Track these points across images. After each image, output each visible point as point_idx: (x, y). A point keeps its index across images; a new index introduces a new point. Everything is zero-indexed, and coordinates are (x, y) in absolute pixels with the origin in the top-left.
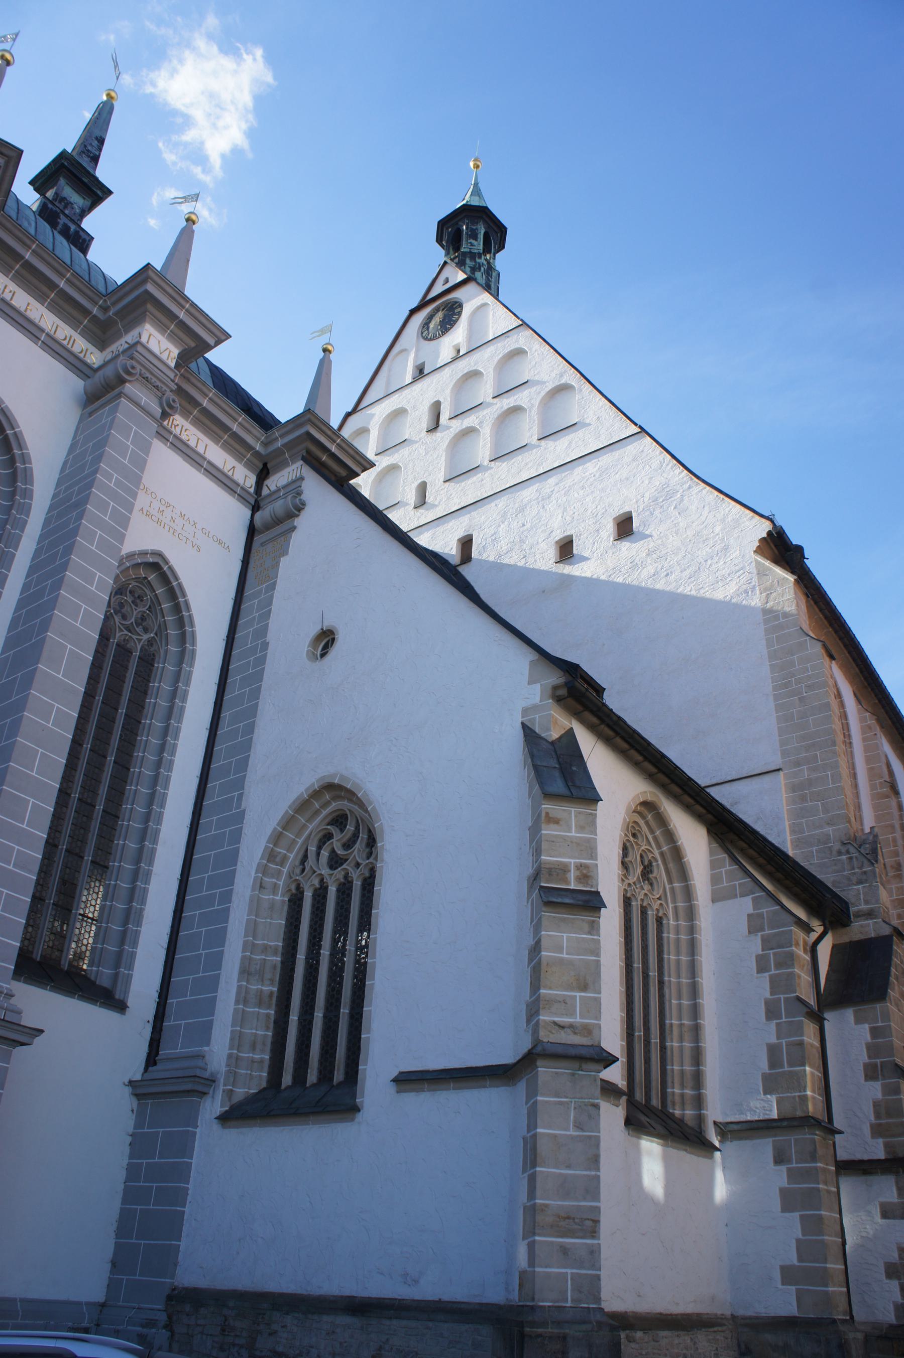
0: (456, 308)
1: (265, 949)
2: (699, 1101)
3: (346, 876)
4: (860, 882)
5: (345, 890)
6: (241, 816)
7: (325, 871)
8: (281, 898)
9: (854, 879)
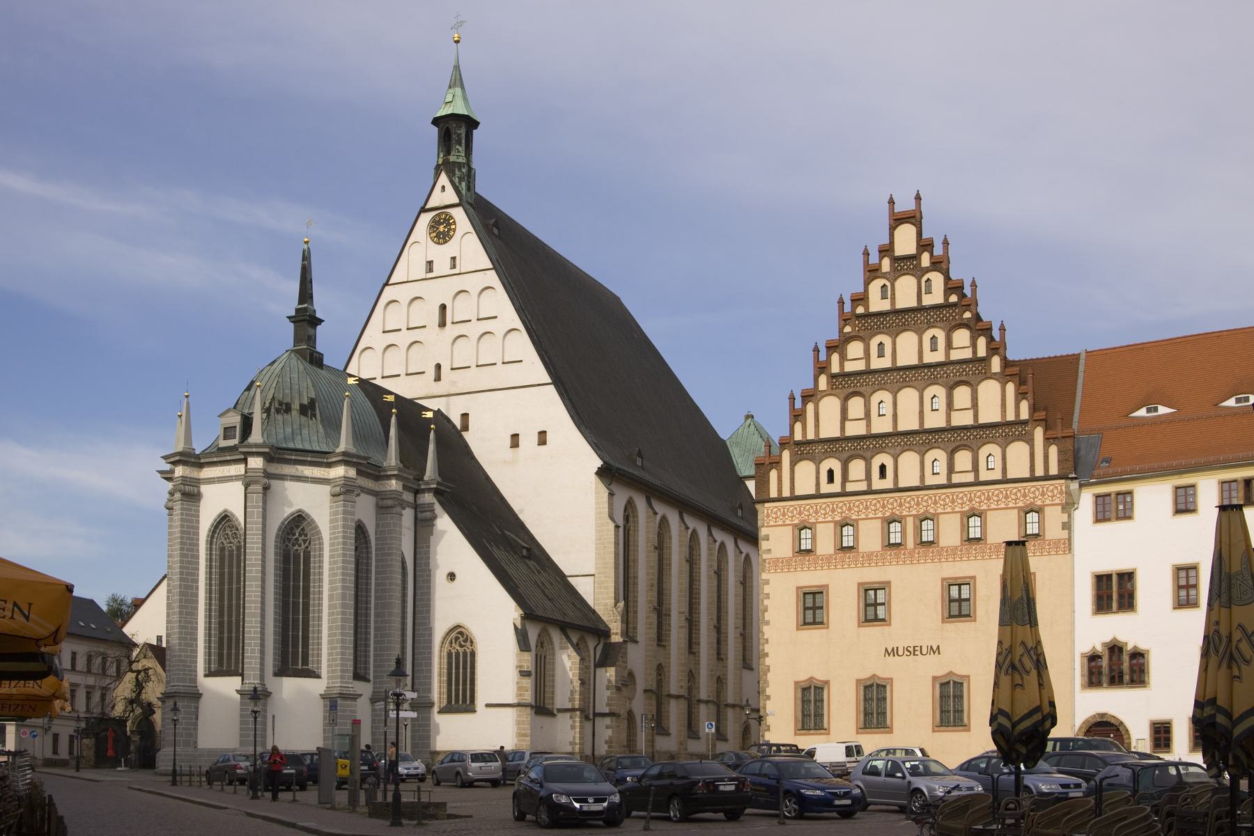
0: (451, 224)
2: (553, 704)
3: (465, 650)
4: (615, 622)
5: (465, 653)
7: (459, 648)
8: (445, 654)
9: (614, 621)
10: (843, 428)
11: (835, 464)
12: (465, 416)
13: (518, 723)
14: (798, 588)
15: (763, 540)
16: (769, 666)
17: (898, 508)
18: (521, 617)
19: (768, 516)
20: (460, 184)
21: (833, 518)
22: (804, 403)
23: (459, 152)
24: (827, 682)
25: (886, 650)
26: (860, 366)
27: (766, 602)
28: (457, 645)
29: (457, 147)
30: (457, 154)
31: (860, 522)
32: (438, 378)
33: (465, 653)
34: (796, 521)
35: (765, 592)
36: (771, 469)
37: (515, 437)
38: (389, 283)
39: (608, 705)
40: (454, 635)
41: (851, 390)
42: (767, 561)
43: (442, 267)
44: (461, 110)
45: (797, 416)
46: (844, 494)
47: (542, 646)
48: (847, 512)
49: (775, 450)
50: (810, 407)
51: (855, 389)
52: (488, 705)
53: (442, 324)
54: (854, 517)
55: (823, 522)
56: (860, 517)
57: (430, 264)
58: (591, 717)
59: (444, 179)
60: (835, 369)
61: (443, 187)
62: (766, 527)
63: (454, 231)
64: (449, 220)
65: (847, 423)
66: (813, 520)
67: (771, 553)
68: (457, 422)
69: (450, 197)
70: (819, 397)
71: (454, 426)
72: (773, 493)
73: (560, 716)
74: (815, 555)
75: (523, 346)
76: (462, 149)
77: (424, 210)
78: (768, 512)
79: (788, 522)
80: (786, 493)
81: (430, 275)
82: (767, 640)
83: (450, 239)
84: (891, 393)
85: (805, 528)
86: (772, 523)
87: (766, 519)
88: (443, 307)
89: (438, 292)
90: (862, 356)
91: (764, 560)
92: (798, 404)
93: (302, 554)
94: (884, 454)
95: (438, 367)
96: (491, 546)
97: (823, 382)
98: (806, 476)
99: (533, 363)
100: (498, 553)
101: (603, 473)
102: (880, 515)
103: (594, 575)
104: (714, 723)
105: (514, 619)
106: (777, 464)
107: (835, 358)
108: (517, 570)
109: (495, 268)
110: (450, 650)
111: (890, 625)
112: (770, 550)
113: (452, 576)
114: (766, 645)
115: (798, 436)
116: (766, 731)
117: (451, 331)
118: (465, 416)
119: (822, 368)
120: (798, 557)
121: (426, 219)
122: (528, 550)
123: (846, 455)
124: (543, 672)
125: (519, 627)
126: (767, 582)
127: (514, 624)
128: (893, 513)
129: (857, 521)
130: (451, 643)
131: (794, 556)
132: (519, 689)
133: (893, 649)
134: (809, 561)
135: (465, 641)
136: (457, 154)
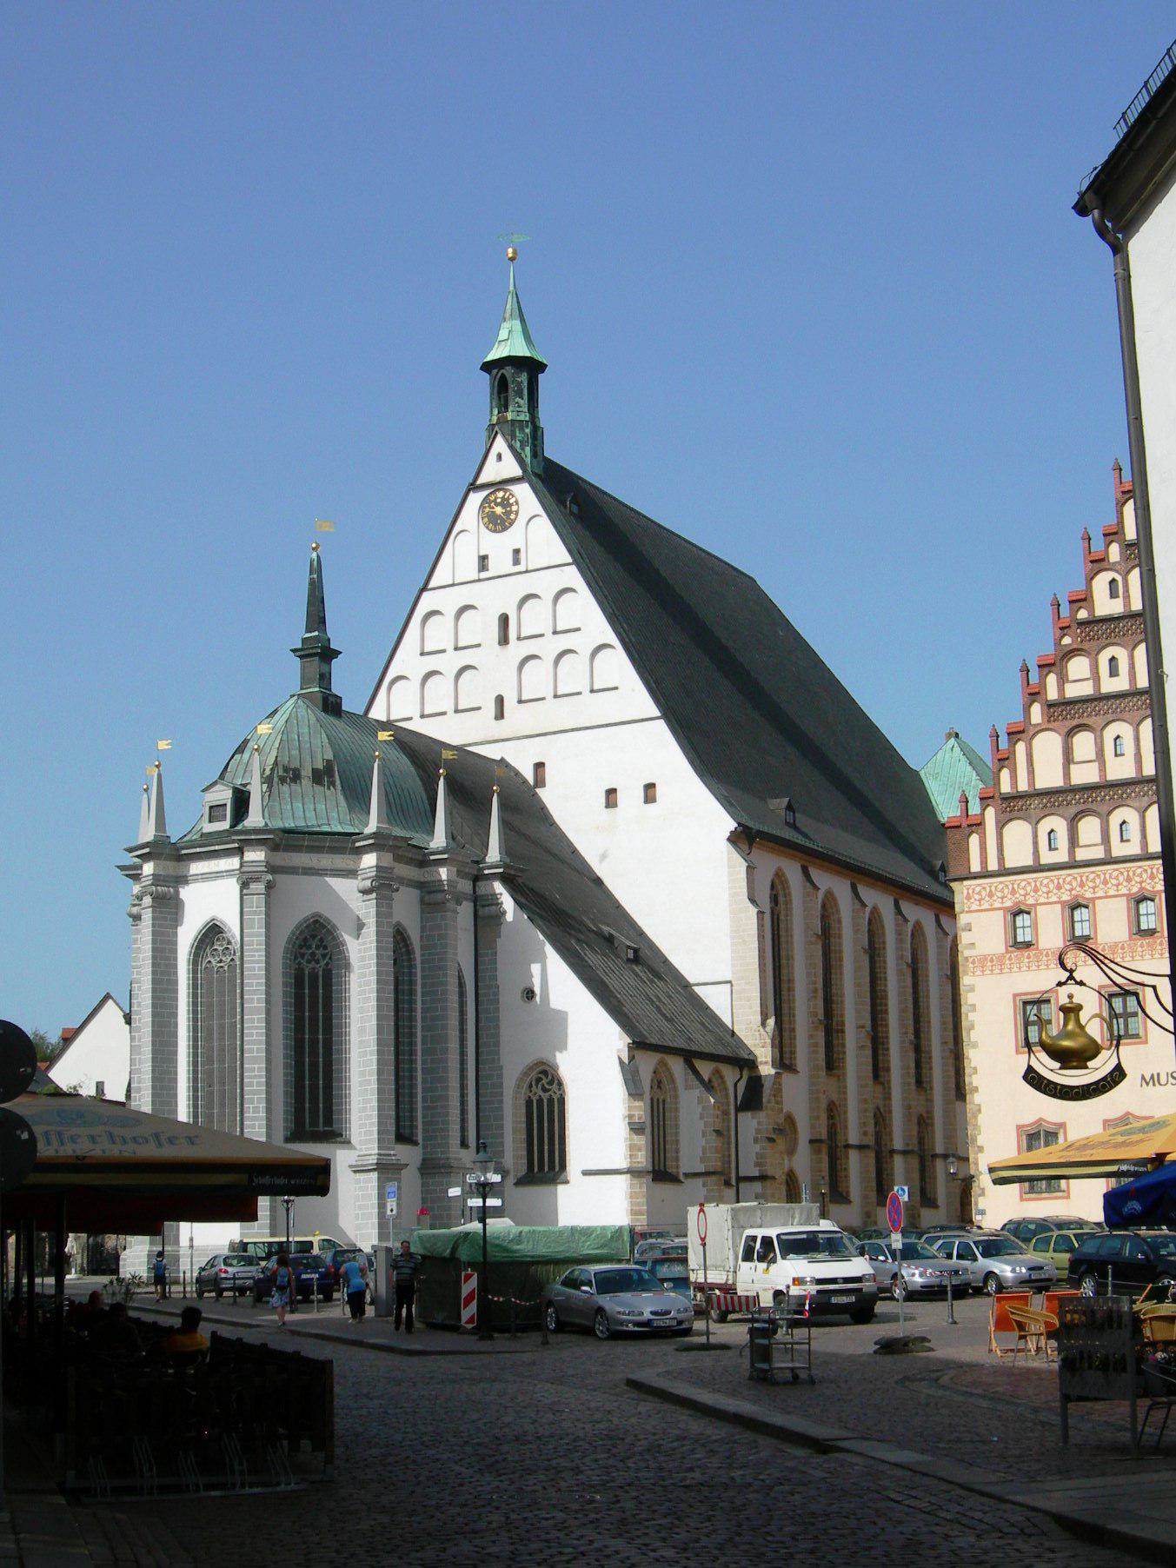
2: (677, 1167)
4: (763, 1047)
6: (501, 1068)
8: (523, 1102)
10: (1067, 774)
11: (1057, 823)
12: (539, 766)
13: (632, 1196)
14: (1015, 996)
15: (963, 930)
16: (979, 1105)
17: (1148, 881)
18: (629, 1047)
19: (968, 897)
20: (523, 449)
21: (1059, 898)
22: (1013, 744)
23: (519, 406)
24: (1062, 1125)
25: (1143, 1078)
26: (1086, 689)
27: (972, 1016)
29: (518, 399)
30: (517, 409)
31: (1097, 902)
32: (500, 715)
34: (1008, 904)
35: (970, 1002)
36: (970, 835)
37: (611, 793)
38: (430, 586)
39: (757, 1164)
40: (533, 1075)
41: (1075, 722)
42: (971, 960)
43: (500, 562)
44: (521, 350)
45: (1005, 760)
46: (1073, 865)
47: (659, 1087)
48: (1078, 889)
49: (975, 808)
50: (1020, 748)
51: (1081, 721)
52: (586, 1173)
53: (504, 640)
54: (1089, 895)
55: (1046, 904)
56: (1097, 895)
57: (483, 561)
58: (734, 1182)
59: (500, 445)
60: (1052, 694)
61: (499, 457)
62: (967, 912)
63: (517, 513)
64: (508, 499)
65: (1072, 766)
66: (1031, 901)
67: (975, 948)
68: (529, 775)
69: (511, 468)
70: (1031, 734)
71: (525, 781)
72: (975, 867)
73: (688, 1182)
74: (1037, 949)
75: (618, 666)
76: (524, 402)
77: (474, 487)
78: (968, 893)
79: (997, 905)
80: (993, 865)
81: (484, 575)
82: (975, 1069)
83: (511, 524)
84: (1131, 724)
85: (1021, 912)
86: (974, 907)
87: (965, 901)
88: (504, 620)
89: (496, 598)
90: (1088, 676)
91: (967, 959)
92: (1003, 743)
93: (321, 973)
94: (1125, 808)
95: (500, 701)
96: (583, 949)
97: (1036, 714)
98: (1018, 841)
99: (633, 690)
100: (592, 958)
101: (734, 839)
102: (1124, 891)
103: (730, 982)
104: (906, 1188)
105: (619, 1050)
106: (978, 825)
107: (1052, 679)
108: (622, 980)
109: (576, 562)
111: (1146, 1042)
112: (973, 944)
114: (973, 1076)
115: (1006, 787)
116: (980, 1196)
117: (517, 650)
118: (539, 766)
119: (1035, 695)
120: (1012, 952)
121: (475, 499)
122: (636, 951)
123: (1073, 810)
124: (661, 1123)
125: (626, 1061)
126: (972, 989)
127: (619, 1058)
128: (1142, 888)
129: (1093, 900)
130: (531, 1086)
131: (1007, 951)
132: (632, 1147)
133: (1152, 1077)
134: (1029, 957)
136: (517, 409)
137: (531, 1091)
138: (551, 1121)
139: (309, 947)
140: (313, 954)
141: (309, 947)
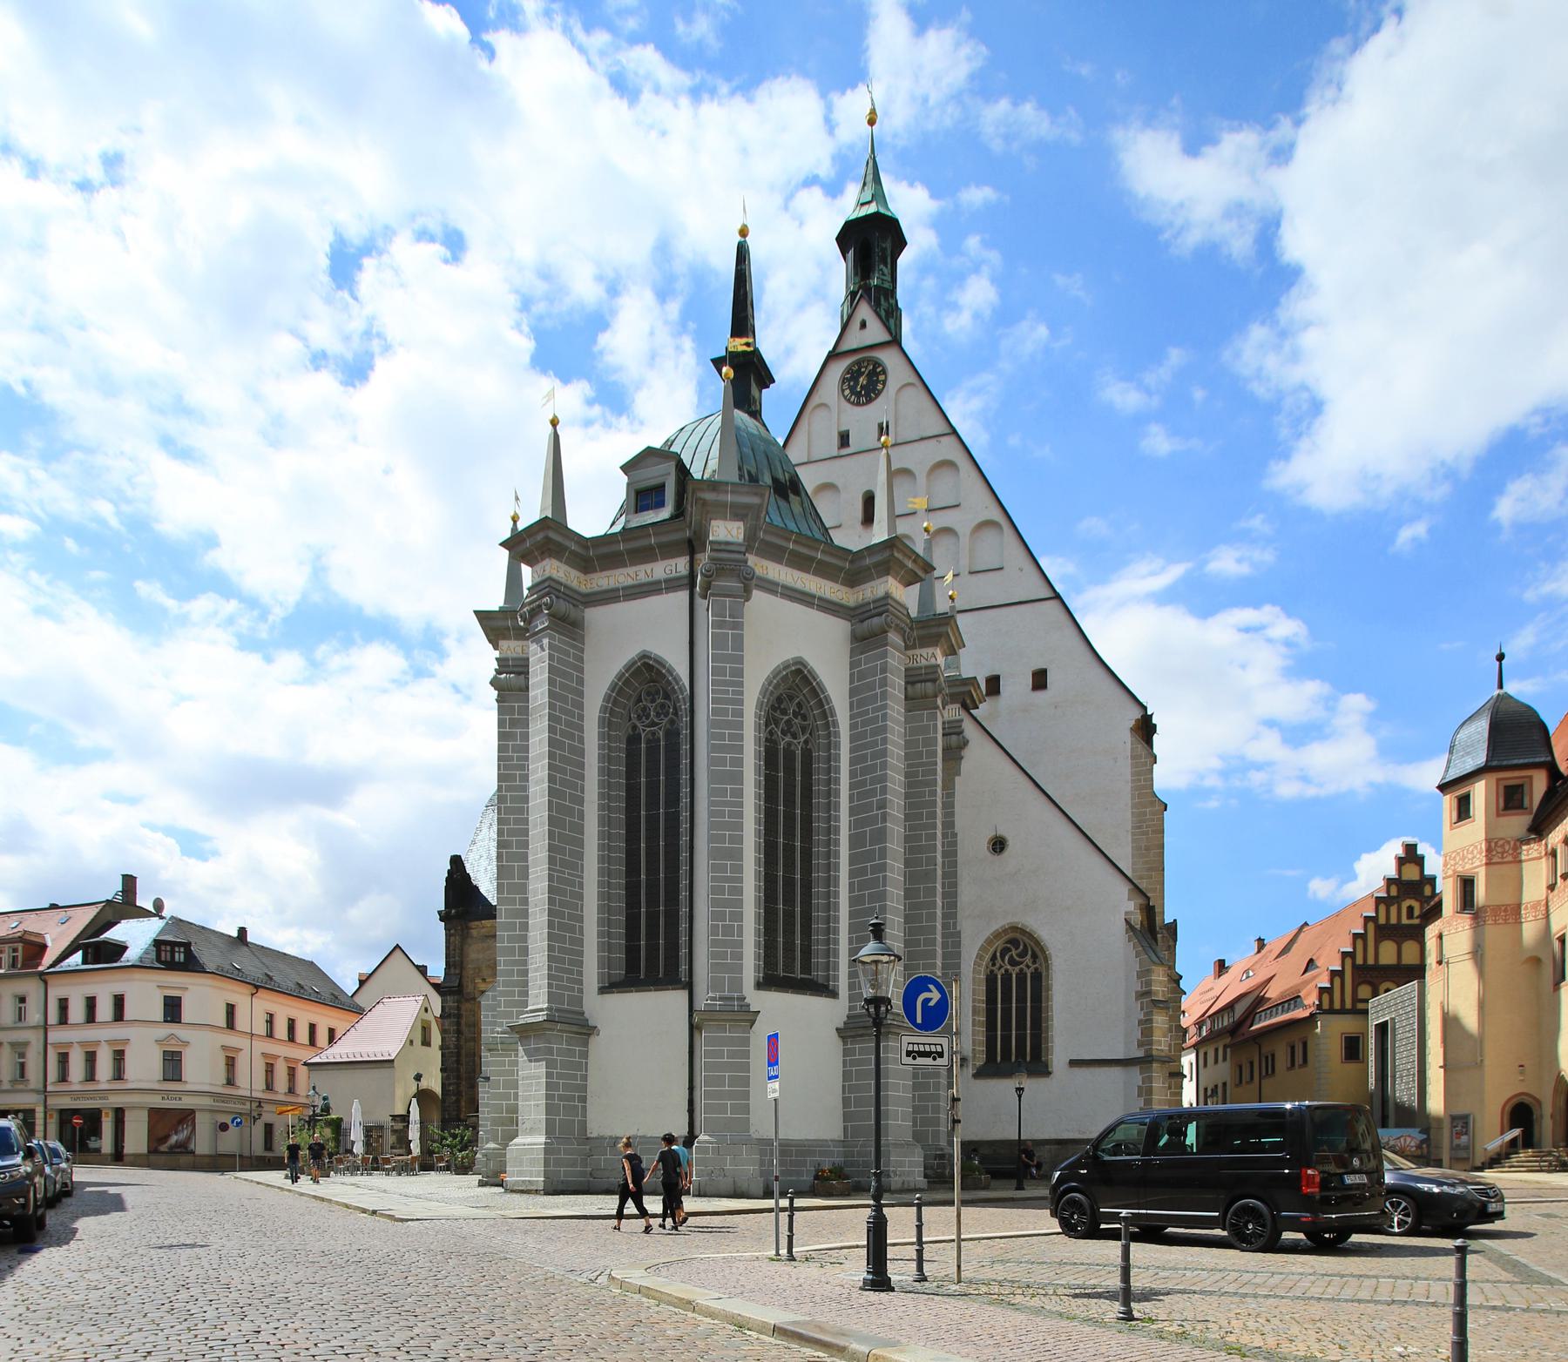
1: (979, 1001)
3: (1021, 970)
5: (1021, 977)
7: (1009, 967)
28: (1006, 961)
33: (1021, 977)
40: (999, 944)
83: (877, 396)
110: (992, 971)
113: (998, 845)
130: (994, 958)
135: (1023, 954)
137: (994, 965)
138: (1021, 999)
139: (784, 712)
140: (788, 722)
141: (784, 712)
